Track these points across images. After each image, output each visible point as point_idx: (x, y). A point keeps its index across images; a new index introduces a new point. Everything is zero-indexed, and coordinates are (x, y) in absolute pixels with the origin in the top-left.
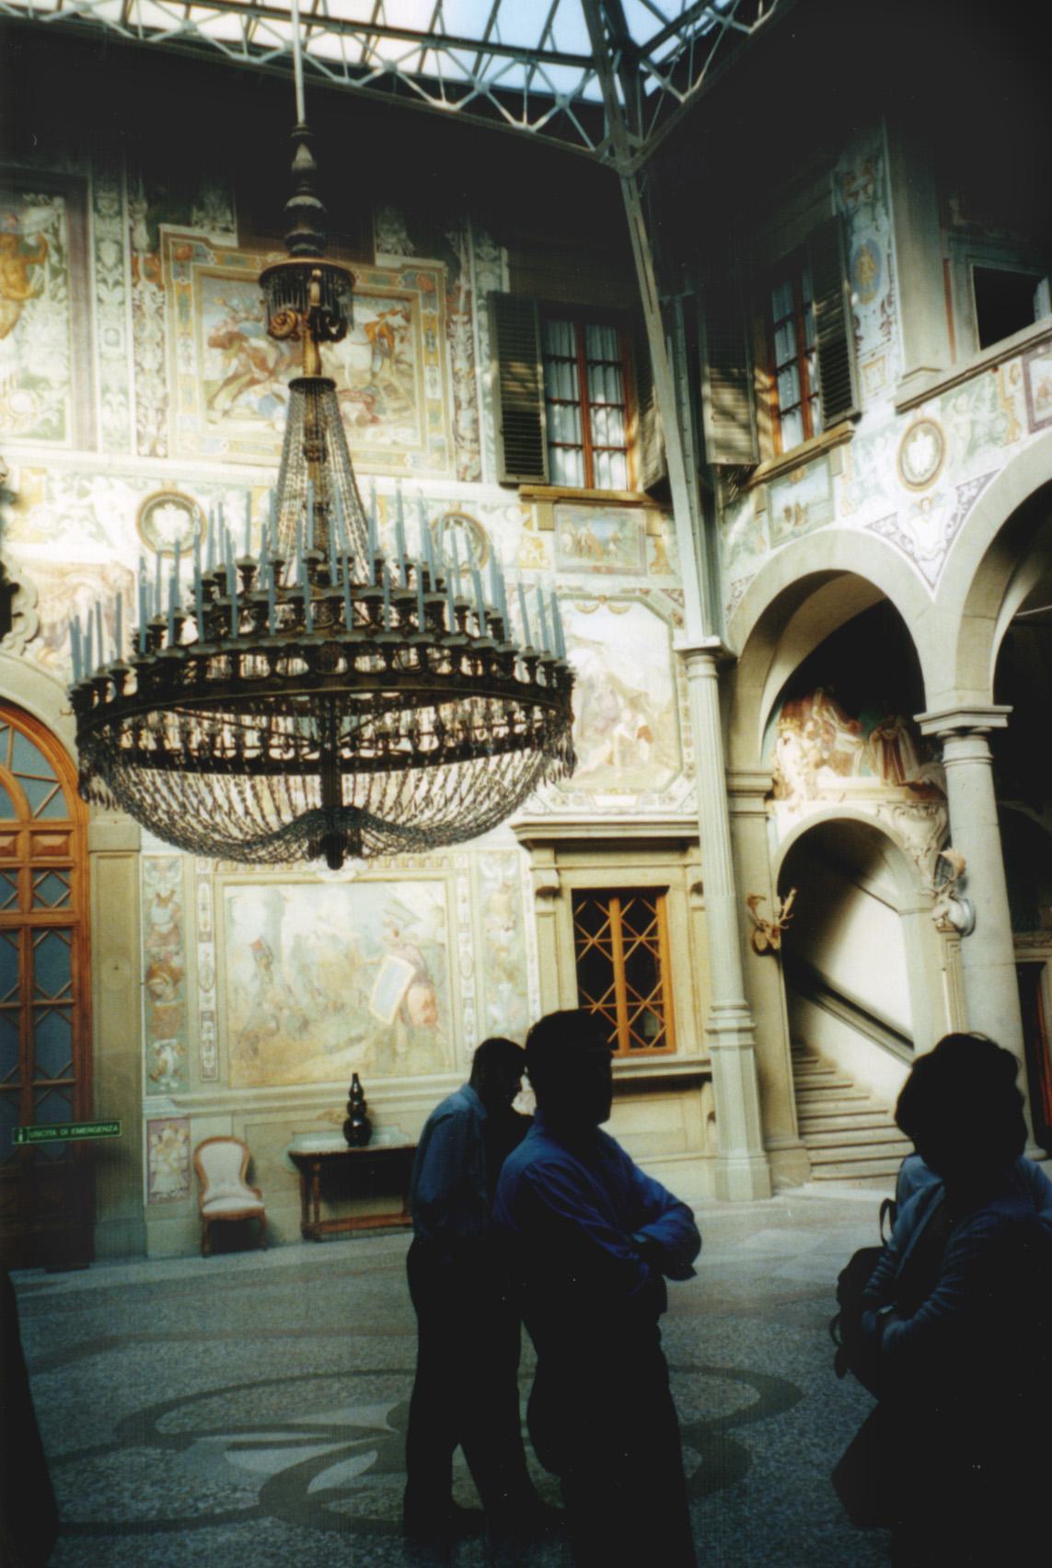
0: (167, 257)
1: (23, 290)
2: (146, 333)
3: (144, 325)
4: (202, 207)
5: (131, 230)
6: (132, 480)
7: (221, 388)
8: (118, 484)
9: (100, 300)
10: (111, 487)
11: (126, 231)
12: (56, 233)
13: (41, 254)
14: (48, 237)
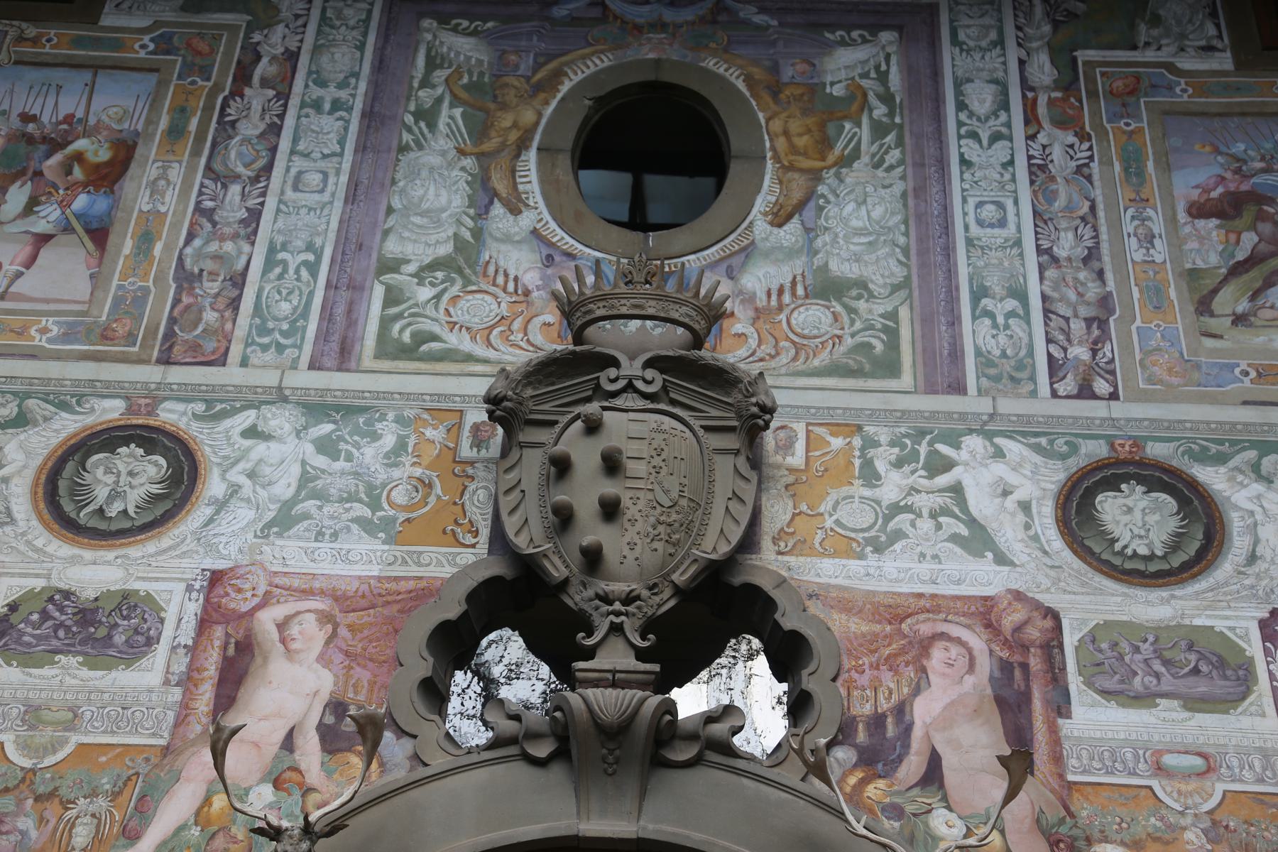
0: (1093, 94)
1: (823, 159)
2: (1060, 203)
3: (1055, 193)
4: (1156, 21)
5: (1022, 63)
6: (1043, 441)
7: (1225, 280)
8: (1012, 447)
9: (965, 163)
10: (999, 454)
11: (1013, 66)
12: (883, 77)
13: (855, 107)
14: (865, 83)
